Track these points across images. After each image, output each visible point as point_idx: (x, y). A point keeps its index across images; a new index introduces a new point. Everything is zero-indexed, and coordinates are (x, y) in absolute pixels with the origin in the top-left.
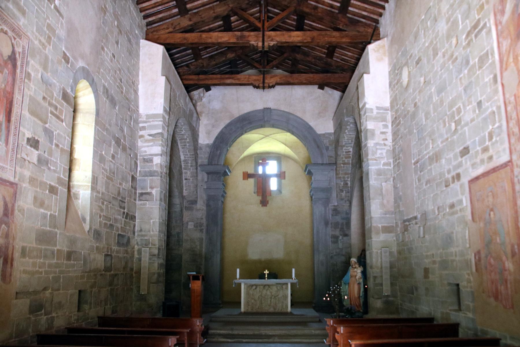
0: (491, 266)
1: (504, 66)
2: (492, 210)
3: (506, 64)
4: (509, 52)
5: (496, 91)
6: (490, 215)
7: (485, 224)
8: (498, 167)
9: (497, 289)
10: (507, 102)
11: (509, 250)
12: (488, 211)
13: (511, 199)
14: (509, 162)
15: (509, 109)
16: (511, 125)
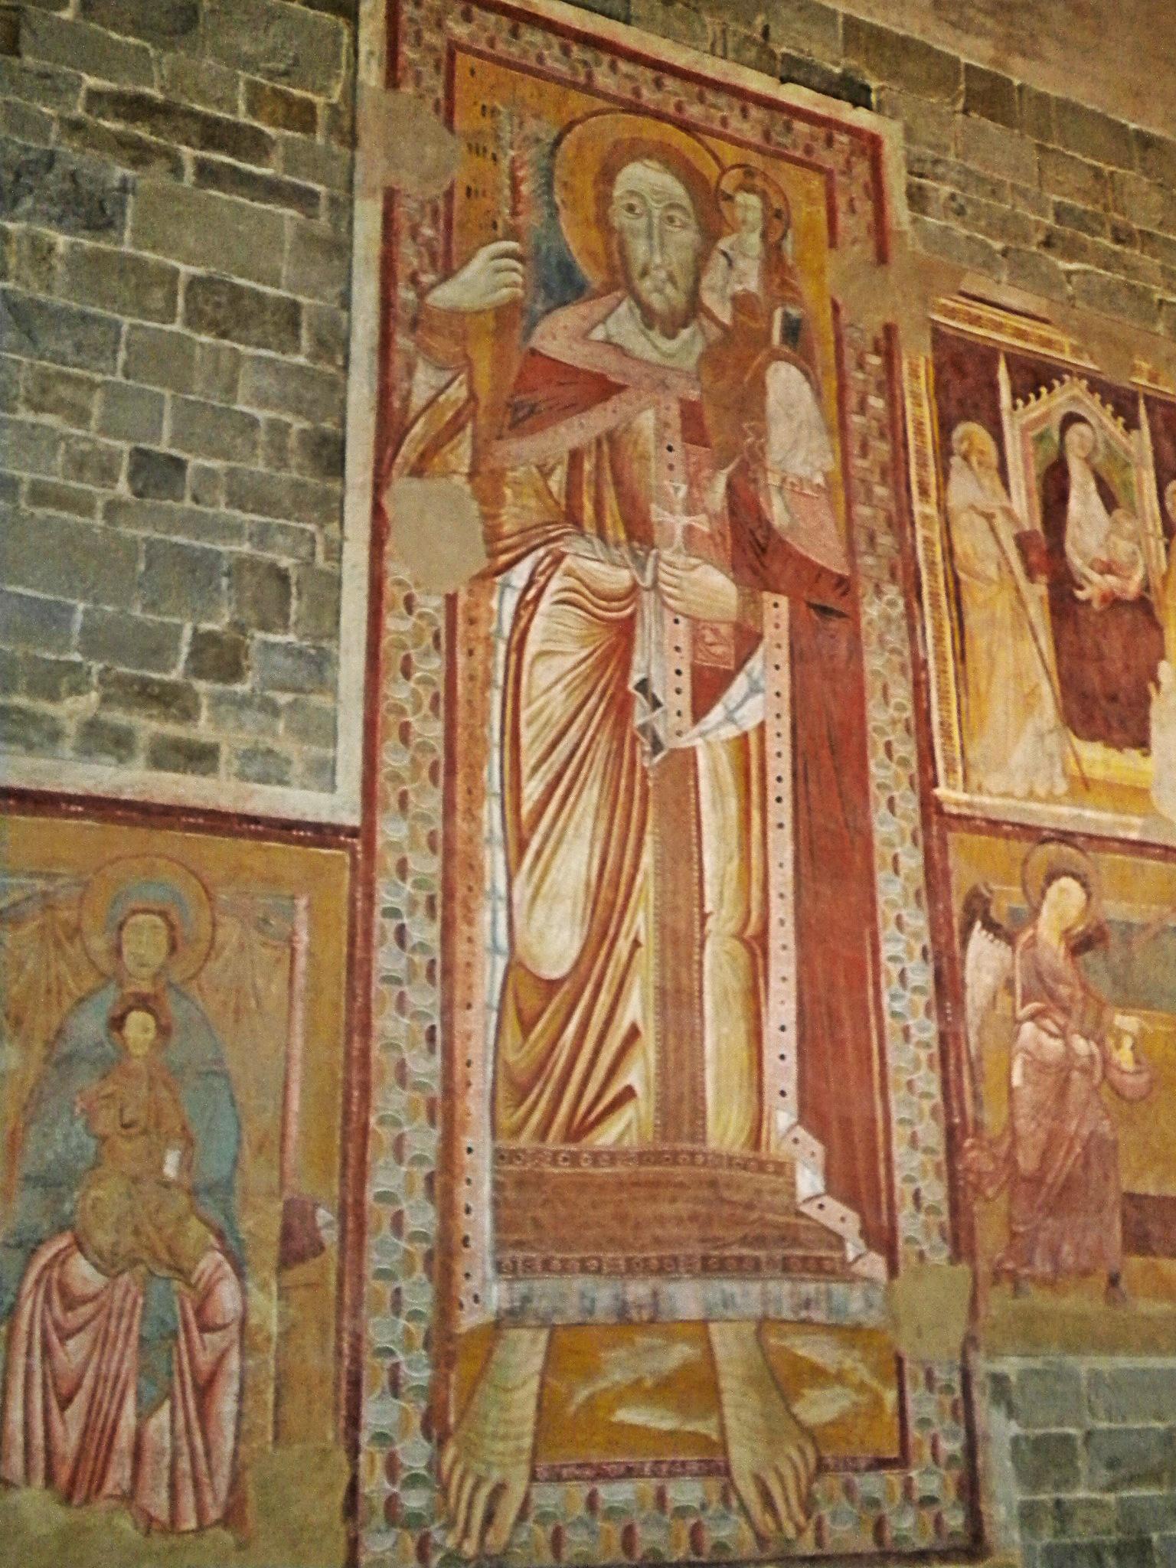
0: (71, 1302)
1: (408, 451)
2: (144, 1003)
3: (423, 456)
4: (455, 427)
5: (332, 509)
6: (117, 1023)
7: (61, 1060)
8: (256, 820)
9: (99, 1436)
10: (390, 589)
11: (261, 1225)
12: (110, 997)
13: (335, 991)
14: (353, 832)
15: (395, 624)
16: (397, 691)
